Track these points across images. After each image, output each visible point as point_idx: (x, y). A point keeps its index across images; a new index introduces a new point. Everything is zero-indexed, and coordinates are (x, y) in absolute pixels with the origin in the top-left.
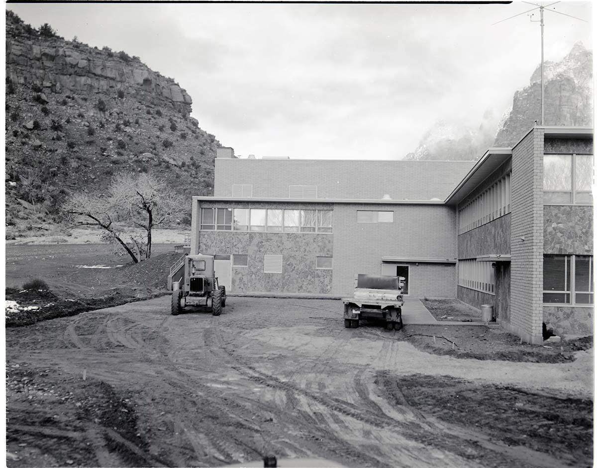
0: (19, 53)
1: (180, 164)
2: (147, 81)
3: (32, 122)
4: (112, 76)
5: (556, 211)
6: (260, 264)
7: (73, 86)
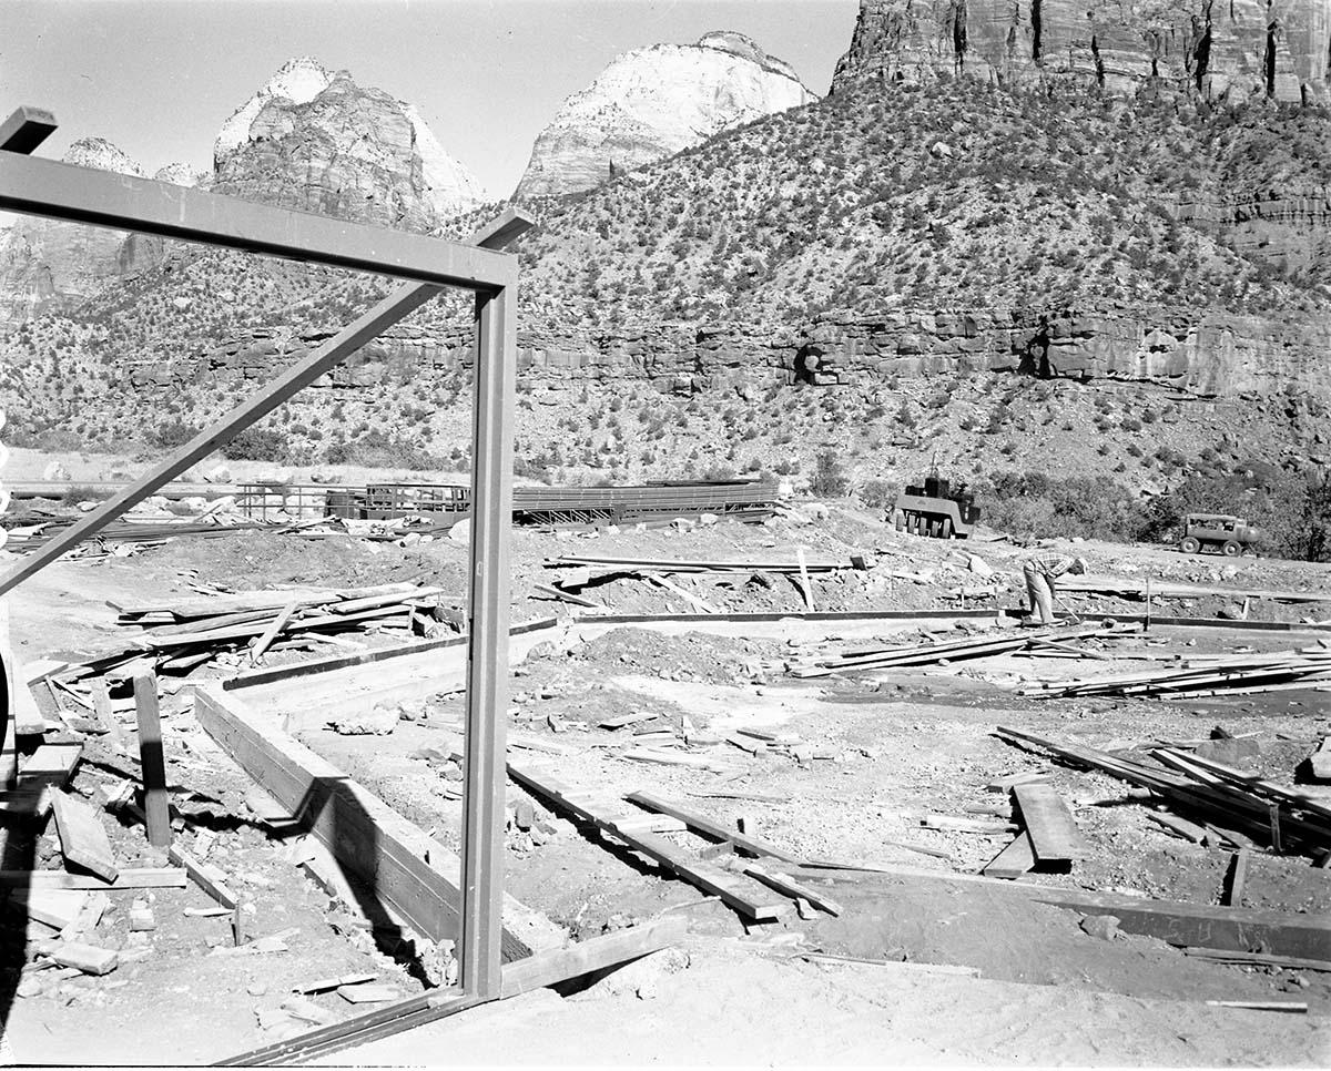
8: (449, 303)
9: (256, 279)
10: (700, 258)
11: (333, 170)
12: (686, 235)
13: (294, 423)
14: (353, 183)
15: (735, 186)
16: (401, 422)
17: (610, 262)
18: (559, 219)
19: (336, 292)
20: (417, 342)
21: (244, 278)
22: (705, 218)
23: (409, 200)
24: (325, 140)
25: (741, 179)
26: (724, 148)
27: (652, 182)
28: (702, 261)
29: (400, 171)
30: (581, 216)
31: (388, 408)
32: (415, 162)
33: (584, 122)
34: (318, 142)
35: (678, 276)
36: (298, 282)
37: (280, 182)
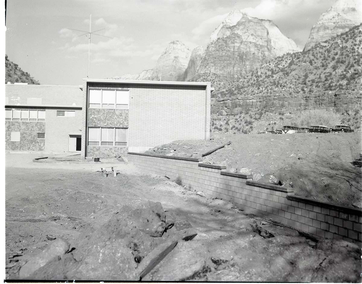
5: (94, 111)
6: (9, 137)
8: (261, 89)
9: (218, 82)
10: (340, 71)
11: (242, 46)
12: (338, 62)
13: (216, 126)
14: (248, 50)
15: (355, 45)
16: (244, 125)
17: (312, 73)
18: (299, 60)
19: (232, 86)
20: (251, 101)
21: (214, 82)
22: (344, 57)
23: (267, 53)
24: (239, 37)
25: (358, 42)
26: (353, 32)
27: (328, 45)
28: (341, 71)
29: (263, 44)
30: (305, 59)
31: (241, 120)
32: (268, 41)
33: (328, 21)
34: (237, 38)
35: (332, 76)
36: (231, 82)
37: (225, 51)
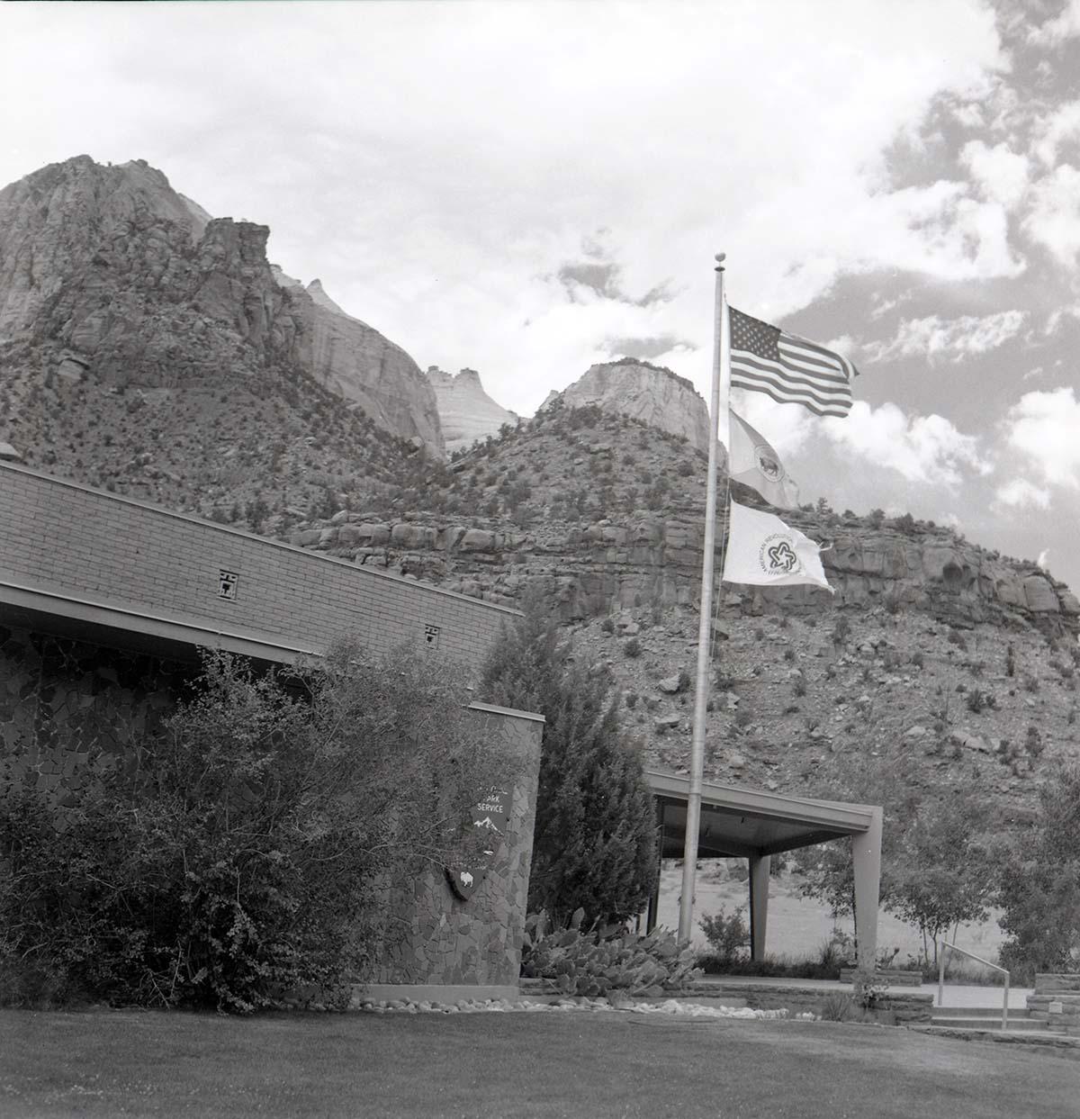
0: (679, 543)
1: (997, 746)
2: (951, 571)
3: (676, 678)
4: (874, 568)
7: (787, 598)
